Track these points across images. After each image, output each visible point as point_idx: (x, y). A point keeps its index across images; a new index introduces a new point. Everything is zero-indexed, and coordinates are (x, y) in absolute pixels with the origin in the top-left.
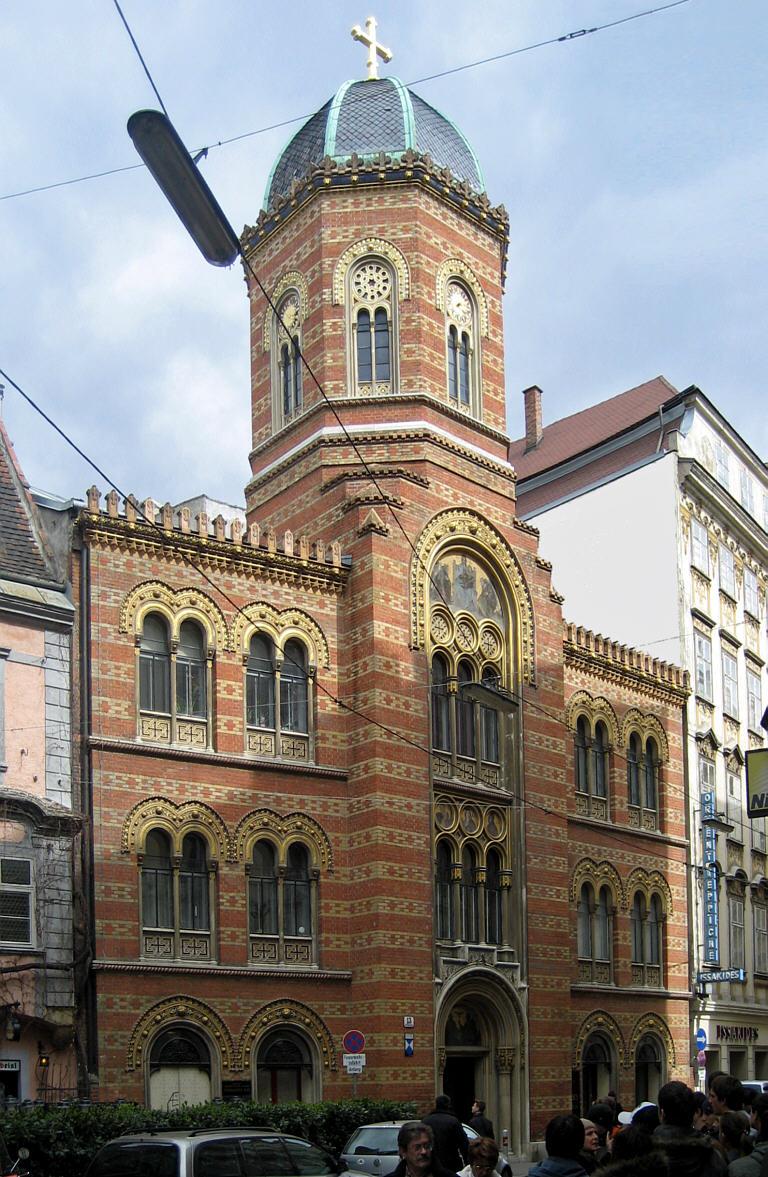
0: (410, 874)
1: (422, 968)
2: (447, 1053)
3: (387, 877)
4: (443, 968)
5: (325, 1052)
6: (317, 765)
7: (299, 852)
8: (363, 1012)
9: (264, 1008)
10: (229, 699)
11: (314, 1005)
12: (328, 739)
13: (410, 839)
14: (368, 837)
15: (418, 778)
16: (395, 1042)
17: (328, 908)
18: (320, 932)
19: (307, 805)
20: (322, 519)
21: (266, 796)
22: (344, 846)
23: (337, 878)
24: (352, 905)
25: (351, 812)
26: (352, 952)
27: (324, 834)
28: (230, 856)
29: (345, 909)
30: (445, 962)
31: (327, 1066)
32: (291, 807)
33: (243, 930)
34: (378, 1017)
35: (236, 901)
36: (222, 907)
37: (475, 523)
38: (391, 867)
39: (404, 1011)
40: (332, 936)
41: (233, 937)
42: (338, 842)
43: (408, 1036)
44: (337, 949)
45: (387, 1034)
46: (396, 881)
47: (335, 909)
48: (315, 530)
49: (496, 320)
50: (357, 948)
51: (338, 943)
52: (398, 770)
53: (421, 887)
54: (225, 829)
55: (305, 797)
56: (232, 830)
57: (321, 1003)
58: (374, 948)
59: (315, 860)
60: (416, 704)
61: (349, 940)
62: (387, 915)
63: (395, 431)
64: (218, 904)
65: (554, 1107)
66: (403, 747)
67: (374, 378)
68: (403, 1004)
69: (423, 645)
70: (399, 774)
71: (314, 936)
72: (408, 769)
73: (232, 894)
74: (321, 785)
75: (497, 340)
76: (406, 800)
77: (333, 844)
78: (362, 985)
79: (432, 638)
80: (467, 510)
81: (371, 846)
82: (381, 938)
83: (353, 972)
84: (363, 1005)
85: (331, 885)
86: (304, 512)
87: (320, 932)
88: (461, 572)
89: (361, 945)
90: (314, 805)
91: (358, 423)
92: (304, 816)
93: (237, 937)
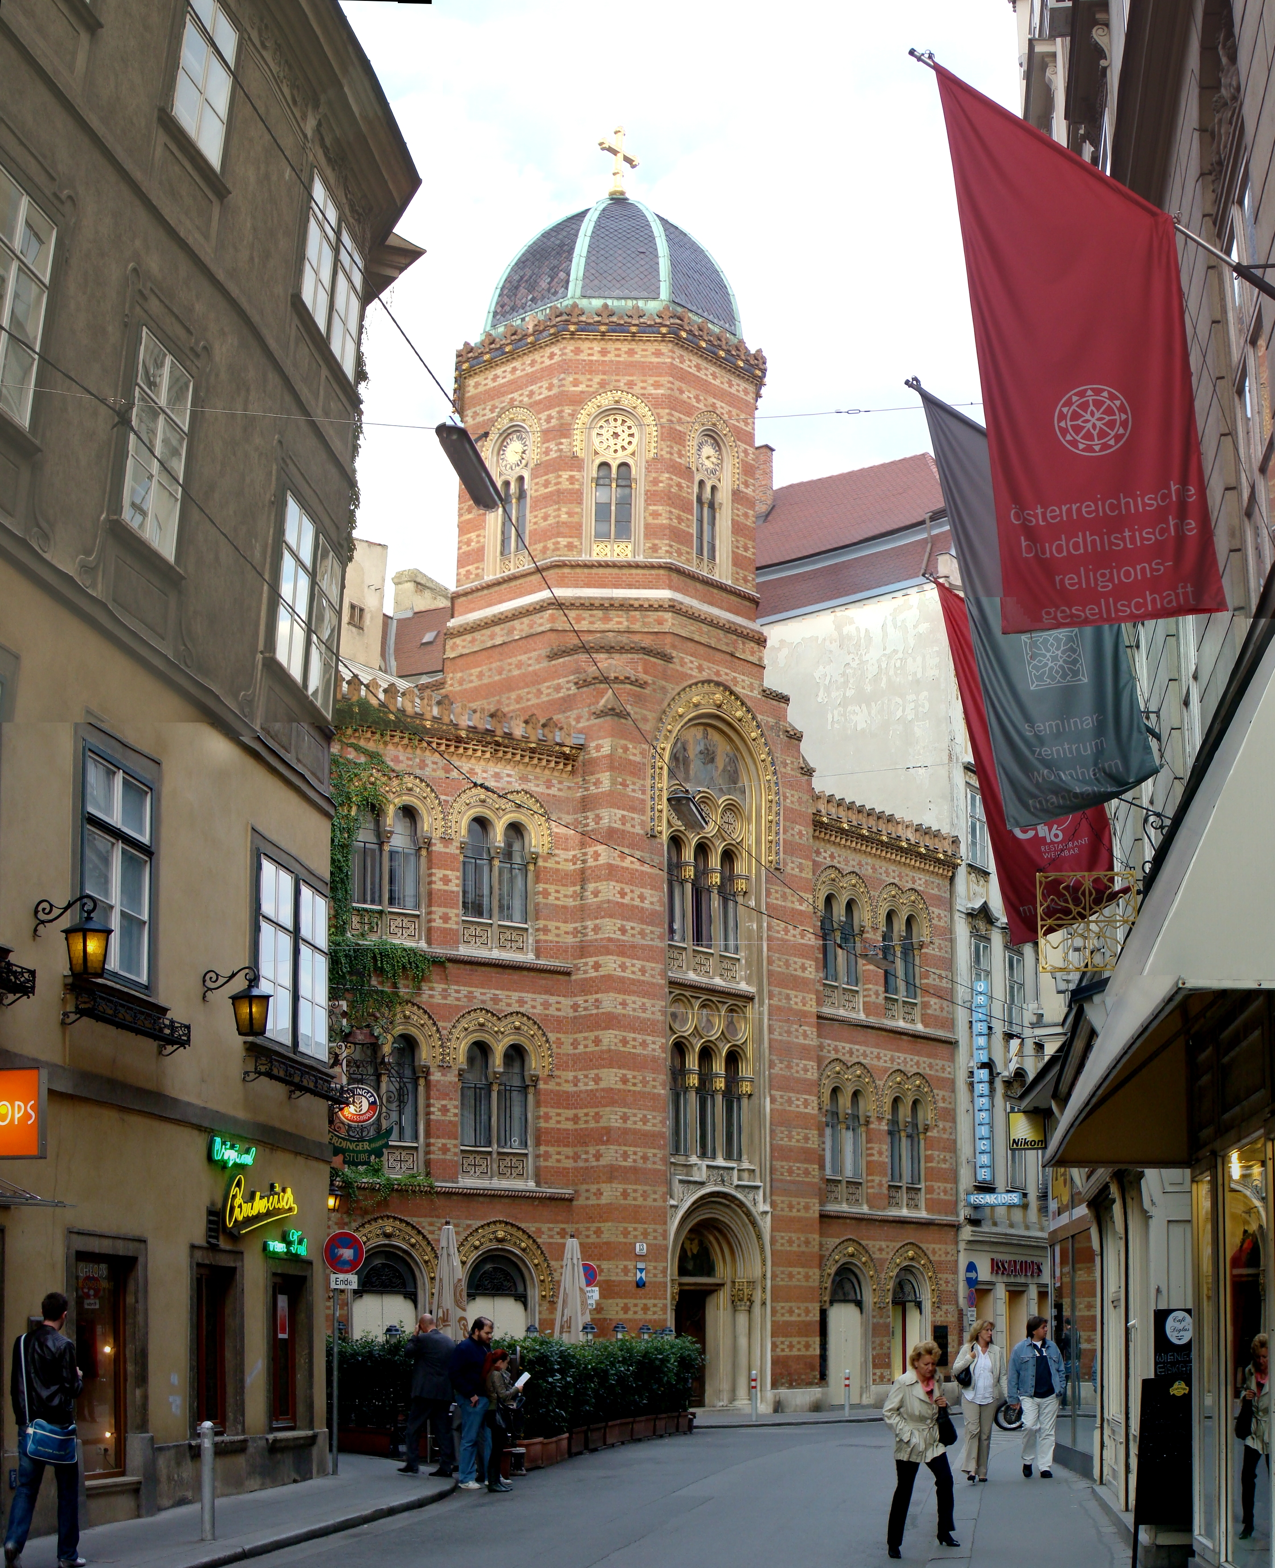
0: (645, 1083)
1: (656, 1188)
2: (680, 1284)
3: (620, 1086)
4: (677, 1188)
5: (542, 1281)
6: (538, 957)
7: (516, 1054)
9: (477, 1230)
11: (531, 1228)
12: (550, 931)
14: (597, 1041)
15: (653, 976)
16: (626, 1270)
17: (547, 1118)
18: (538, 1144)
20: (548, 688)
22: (568, 1049)
23: (559, 1084)
24: (576, 1116)
25: (576, 1011)
26: (575, 1169)
27: (544, 1034)
28: (442, 1061)
29: (567, 1119)
30: (681, 1181)
31: (544, 1297)
32: (509, 1005)
33: (454, 1142)
34: (607, 1244)
35: (448, 1110)
36: (432, 1117)
38: (624, 1075)
39: (635, 1237)
40: (551, 1149)
41: (445, 1149)
43: (641, 1265)
44: (558, 1165)
48: (538, 697)
50: (581, 1164)
51: (558, 1157)
52: (633, 969)
53: (655, 1097)
54: (438, 1031)
55: (523, 995)
56: (444, 1032)
57: (537, 1225)
58: (604, 1166)
59: (536, 1064)
60: (652, 896)
61: (571, 1154)
63: (637, 599)
64: (428, 1114)
68: (635, 1229)
69: (661, 833)
70: (633, 973)
71: (531, 1149)
72: (643, 967)
73: (444, 1102)
74: (544, 981)
76: (639, 1001)
77: (554, 1046)
78: (587, 1206)
79: (669, 821)
81: (602, 1052)
82: (611, 1154)
83: (576, 1191)
84: (588, 1229)
85: (552, 1091)
87: (538, 1144)
88: (702, 747)
89: (586, 1160)
92: (523, 1015)
93: (449, 1150)
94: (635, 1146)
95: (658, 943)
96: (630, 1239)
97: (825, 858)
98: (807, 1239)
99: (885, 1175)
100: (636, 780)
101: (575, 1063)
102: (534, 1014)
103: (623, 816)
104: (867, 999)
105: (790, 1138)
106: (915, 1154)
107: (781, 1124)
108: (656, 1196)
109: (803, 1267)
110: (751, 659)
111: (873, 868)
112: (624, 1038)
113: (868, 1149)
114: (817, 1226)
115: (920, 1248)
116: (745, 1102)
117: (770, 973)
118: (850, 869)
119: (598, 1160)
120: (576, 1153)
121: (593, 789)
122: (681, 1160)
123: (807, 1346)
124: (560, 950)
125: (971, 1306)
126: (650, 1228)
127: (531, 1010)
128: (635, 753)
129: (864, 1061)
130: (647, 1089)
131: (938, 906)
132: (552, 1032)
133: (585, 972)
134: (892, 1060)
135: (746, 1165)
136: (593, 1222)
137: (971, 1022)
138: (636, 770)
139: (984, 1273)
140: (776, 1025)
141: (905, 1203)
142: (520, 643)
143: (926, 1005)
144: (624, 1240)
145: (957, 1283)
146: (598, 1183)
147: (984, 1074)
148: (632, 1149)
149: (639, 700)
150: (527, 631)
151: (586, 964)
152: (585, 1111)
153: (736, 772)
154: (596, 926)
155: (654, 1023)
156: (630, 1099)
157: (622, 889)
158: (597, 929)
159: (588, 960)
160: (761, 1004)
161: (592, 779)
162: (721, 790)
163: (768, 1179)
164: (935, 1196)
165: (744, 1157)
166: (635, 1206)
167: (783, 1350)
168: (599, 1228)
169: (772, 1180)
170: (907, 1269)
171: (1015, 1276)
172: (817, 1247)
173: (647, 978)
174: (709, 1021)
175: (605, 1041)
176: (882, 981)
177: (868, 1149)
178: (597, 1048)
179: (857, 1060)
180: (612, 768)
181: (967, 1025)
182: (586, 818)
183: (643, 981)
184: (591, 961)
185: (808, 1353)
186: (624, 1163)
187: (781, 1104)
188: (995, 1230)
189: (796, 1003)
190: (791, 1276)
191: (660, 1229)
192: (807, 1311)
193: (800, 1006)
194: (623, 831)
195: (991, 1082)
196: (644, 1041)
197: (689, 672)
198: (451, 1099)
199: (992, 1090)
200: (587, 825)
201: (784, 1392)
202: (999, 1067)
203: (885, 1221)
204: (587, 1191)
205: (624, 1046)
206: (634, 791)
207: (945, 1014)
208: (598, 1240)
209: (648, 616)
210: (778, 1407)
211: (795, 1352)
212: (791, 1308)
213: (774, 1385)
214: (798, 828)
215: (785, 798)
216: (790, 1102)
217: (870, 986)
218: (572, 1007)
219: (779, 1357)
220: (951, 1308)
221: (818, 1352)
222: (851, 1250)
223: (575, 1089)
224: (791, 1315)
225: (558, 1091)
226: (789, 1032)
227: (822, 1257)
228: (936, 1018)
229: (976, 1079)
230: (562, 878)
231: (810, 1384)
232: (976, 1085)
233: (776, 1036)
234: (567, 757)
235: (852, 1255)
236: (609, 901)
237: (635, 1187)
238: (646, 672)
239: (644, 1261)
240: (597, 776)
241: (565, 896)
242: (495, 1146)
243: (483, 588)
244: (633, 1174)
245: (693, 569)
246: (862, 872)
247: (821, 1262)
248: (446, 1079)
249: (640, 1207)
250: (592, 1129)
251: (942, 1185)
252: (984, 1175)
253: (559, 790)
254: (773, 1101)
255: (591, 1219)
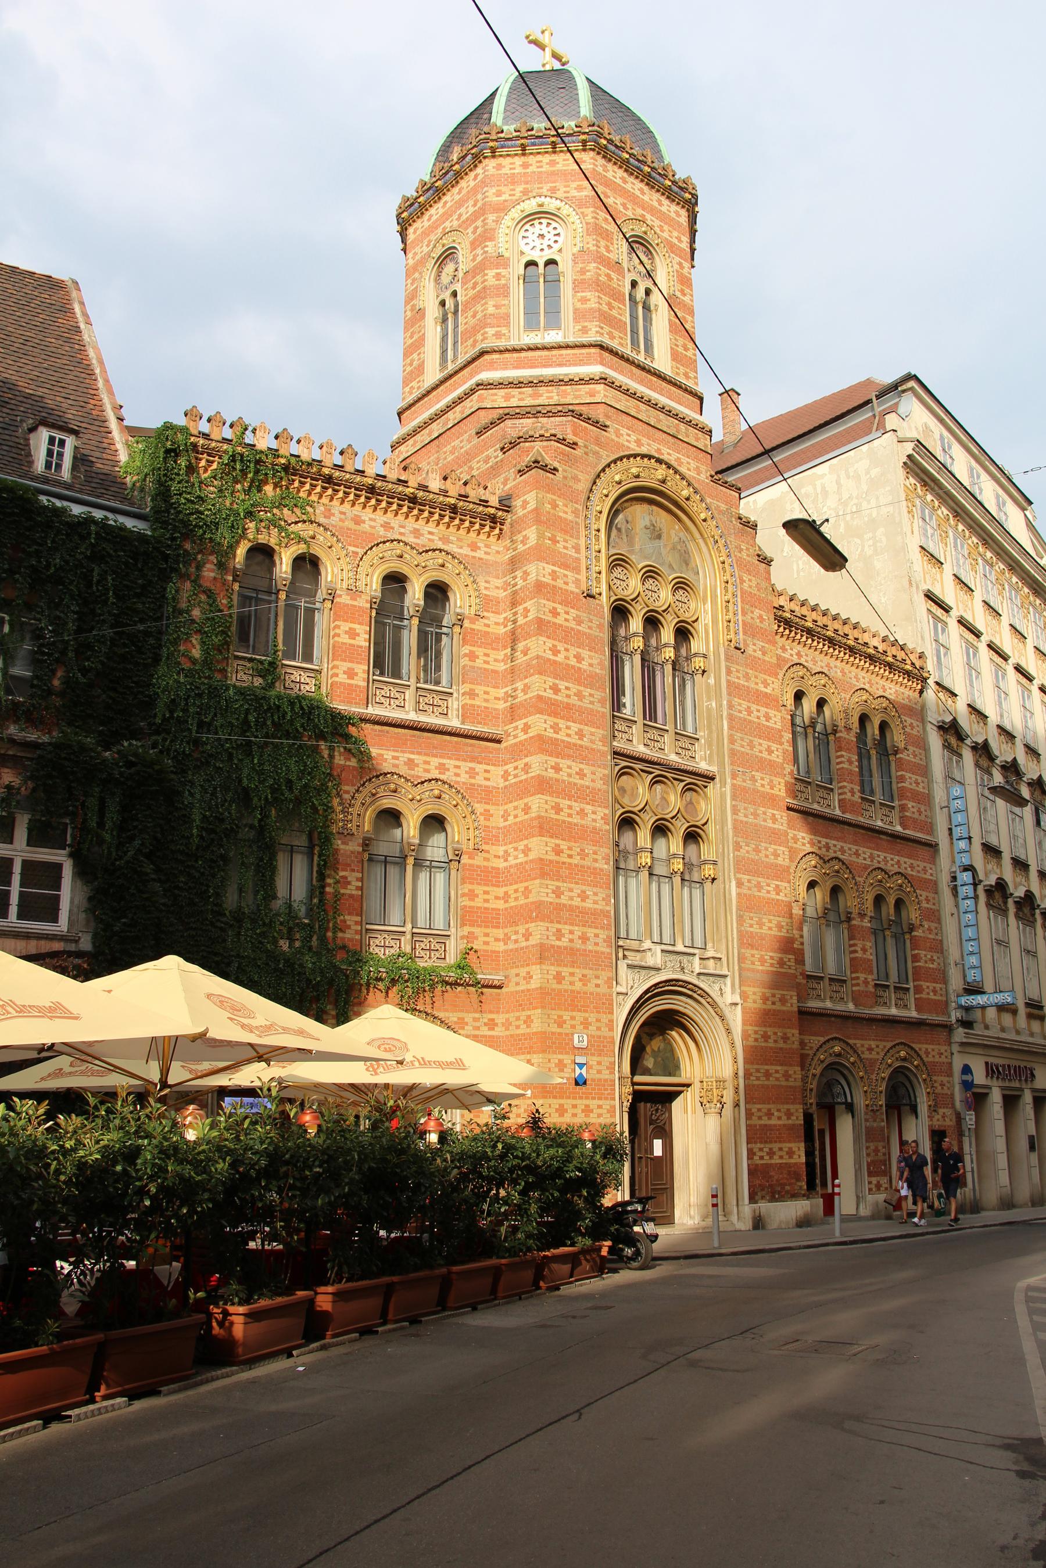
0: (583, 854)
1: (599, 973)
2: (633, 1084)
3: (552, 857)
6: (463, 723)
8: (518, 1027)
10: (350, 645)
12: (478, 695)
13: (582, 813)
15: (593, 742)
17: (472, 895)
19: (448, 770)
20: (478, 462)
21: (395, 758)
22: (497, 822)
23: (485, 859)
24: (506, 893)
26: (506, 951)
28: (344, 827)
29: (497, 898)
32: (427, 771)
37: (661, 472)
39: (573, 1027)
40: (477, 931)
42: (488, 815)
45: (551, 1056)
46: (564, 863)
47: (482, 897)
49: (685, 282)
50: (511, 946)
51: (486, 939)
52: (568, 731)
53: (595, 872)
55: (445, 761)
56: (346, 796)
57: (460, 1015)
58: (533, 946)
61: (501, 937)
62: (551, 903)
65: (781, 1157)
66: (574, 705)
67: (542, 325)
68: (573, 1018)
70: (568, 735)
72: (580, 730)
75: (686, 299)
76: (576, 767)
78: (517, 992)
80: (654, 457)
81: (532, 819)
84: (518, 1019)
85: (478, 867)
86: (457, 457)
89: (516, 941)
90: (457, 771)
91: (524, 368)
92: (444, 783)
94: (572, 924)
95: (597, 707)
96: (566, 1029)
97: (792, 655)
98: (785, 1034)
99: (871, 972)
100: (568, 538)
101: (505, 836)
102: (457, 782)
103: (554, 572)
104: (841, 797)
105: (761, 924)
106: (901, 954)
107: (749, 909)
108: (599, 982)
109: (781, 1065)
110: (695, 444)
111: (842, 671)
112: (557, 804)
113: (851, 946)
114: (795, 1020)
115: (912, 1048)
116: (708, 885)
117: (733, 753)
118: (819, 670)
119: (527, 940)
120: (506, 934)
121: (521, 548)
122: (634, 945)
123: (790, 1153)
124: (487, 714)
125: (969, 1109)
126: (592, 1017)
127: (454, 778)
128: (566, 511)
129: (841, 857)
130: (587, 862)
131: (910, 716)
132: (478, 802)
133: (515, 737)
134: (872, 857)
135: (710, 953)
136: (523, 1010)
137: (950, 829)
138: (568, 529)
139: (979, 1077)
140: (741, 806)
141: (893, 1002)
142: (453, 430)
143: (903, 808)
144: (559, 1030)
145: (953, 1086)
146: (528, 965)
147: (966, 877)
148: (566, 927)
149: (568, 460)
150: (459, 417)
151: (516, 728)
152: (515, 887)
153: (686, 552)
154: (526, 685)
155: (594, 792)
156: (565, 872)
157: (554, 646)
158: (526, 689)
159: (518, 723)
160: (723, 784)
161: (520, 537)
162: (670, 566)
163: (736, 968)
164: (924, 996)
165: (709, 945)
166: (573, 991)
167: (762, 1158)
168: (529, 1017)
169: (740, 969)
170: (899, 1072)
171: (1010, 1080)
172: (796, 1045)
173: (585, 742)
174: (663, 798)
175: (534, 808)
176: (857, 779)
177: (851, 946)
178: (526, 817)
179: (834, 855)
180: (538, 521)
181: (947, 833)
182: (515, 578)
183: (581, 746)
184: (520, 724)
185: (792, 1161)
186: (558, 943)
187: (750, 889)
188: (986, 1033)
189: (763, 786)
190: (767, 1075)
191: (605, 1018)
192: (789, 1115)
193: (767, 789)
194: (555, 587)
195: (975, 885)
196: (582, 810)
197: (626, 443)
198: (353, 870)
199: (976, 897)
200: (515, 585)
201: (765, 1207)
202: (981, 876)
203: (872, 1020)
204: (517, 975)
205: (557, 813)
206: (565, 548)
207: (923, 817)
208: (528, 1030)
209: (579, 390)
210: (758, 1223)
211: (776, 1160)
212: (769, 1110)
213: (752, 1199)
214: (757, 612)
215: (742, 581)
216: (759, 887)
217: (845, 784)
218: (502, 777)
219: (757, 1165)
220: (948, 1112)
221: (803, 1159)
222: (837, 1049)
223: (505, 864)
224: (769, 1119)
225: (486, 867)
226: (756, 815)
227: (803, 1058)
228: (915, 821)
229: (959, 882)
230: (490, 641)
231: (794, 1196)
232: (959, 889)
233: (741, 817)
234: (493, 519)
235: (839, 1055)
236: (538, 657)
237: (571, 970)
238: (575, 434)
239: (586, 1054)
240: (524, 533)
241: (496, 660)
242: (409, 926)
243: (424, 396)
244: (570, 956)
245: (628, 351)
246: (832, 674)
247: (803, 1061)
248: (347, 848)
249: (578, 993)
250: (521, 906)
251: (932, 985)
252: (972, 975)
253: (486, 553)
254: (740, 884)
255: (521, 1007)
